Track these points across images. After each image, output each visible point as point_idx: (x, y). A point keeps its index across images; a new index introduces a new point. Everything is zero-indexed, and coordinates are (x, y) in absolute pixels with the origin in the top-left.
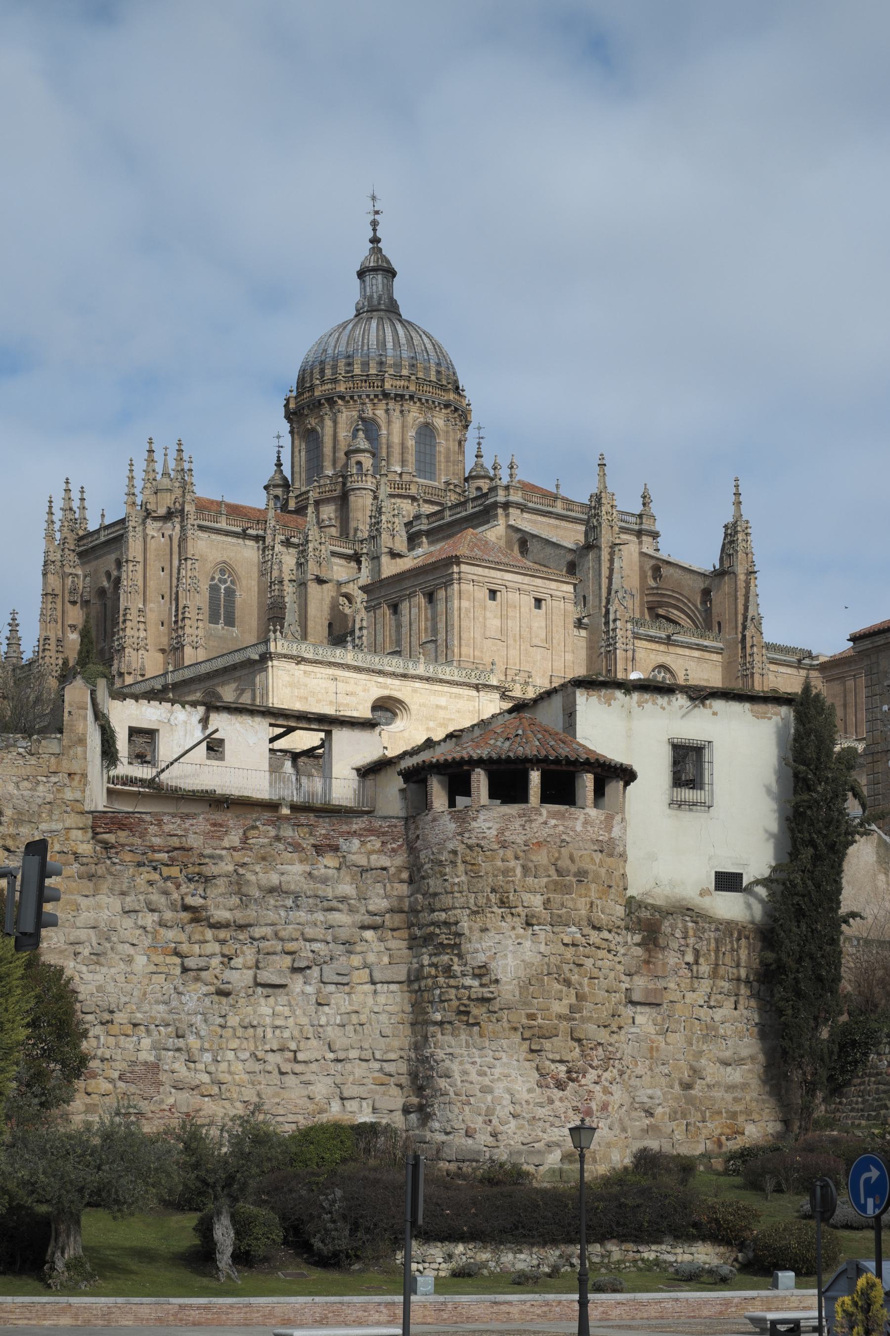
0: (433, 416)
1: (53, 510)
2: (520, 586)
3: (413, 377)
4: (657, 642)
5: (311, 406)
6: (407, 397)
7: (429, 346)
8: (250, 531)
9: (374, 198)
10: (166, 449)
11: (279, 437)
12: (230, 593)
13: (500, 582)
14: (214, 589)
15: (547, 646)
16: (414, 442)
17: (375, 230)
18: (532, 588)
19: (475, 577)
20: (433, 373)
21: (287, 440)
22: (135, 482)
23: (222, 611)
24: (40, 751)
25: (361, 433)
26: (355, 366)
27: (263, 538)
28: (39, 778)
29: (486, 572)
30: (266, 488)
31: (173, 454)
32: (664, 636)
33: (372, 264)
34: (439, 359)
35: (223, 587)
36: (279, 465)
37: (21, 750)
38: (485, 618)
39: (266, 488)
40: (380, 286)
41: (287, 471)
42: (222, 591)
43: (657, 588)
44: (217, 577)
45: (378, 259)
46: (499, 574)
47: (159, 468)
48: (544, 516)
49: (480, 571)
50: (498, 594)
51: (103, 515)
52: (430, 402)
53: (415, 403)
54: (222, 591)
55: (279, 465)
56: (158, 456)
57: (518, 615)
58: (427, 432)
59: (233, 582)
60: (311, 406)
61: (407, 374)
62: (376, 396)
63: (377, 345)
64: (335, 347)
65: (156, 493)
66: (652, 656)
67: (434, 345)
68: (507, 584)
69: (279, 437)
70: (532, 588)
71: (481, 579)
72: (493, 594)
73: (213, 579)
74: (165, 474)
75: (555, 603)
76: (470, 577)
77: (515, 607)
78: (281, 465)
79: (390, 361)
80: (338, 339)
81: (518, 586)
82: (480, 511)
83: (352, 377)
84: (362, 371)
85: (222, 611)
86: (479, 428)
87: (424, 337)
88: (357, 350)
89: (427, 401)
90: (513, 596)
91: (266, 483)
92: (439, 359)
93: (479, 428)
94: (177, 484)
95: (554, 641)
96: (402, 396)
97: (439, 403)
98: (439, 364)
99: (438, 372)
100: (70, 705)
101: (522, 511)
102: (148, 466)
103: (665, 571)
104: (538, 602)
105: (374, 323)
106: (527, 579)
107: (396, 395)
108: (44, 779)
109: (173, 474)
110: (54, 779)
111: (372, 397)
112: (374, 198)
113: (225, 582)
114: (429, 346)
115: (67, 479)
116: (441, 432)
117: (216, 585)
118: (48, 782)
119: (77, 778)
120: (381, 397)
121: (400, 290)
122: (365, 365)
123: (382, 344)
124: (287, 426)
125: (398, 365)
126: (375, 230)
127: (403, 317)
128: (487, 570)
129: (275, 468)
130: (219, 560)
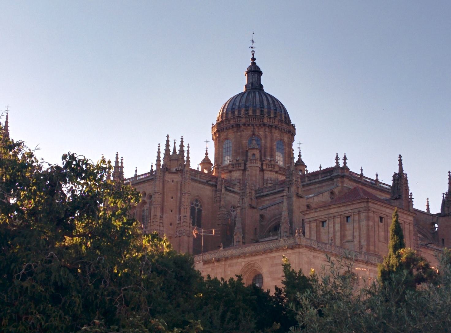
6: (274, 127)
7: (281, 105)
9: (253, 41)
12: (200, 211)
13: (384, 213)
17: (253, 55)
22: (160, 155)
26: (250, 111)
27: (216, 186)
33: (253, 69)
35: (197, 208)
36: (207, 154)
42: (196, 210)
47: (171, 149)
51: (136, 171)
54: (196, 210)
55: (207, 154)
56: (171, 144)
59: (201, 206)
64: (240, 103)
65: (170, 161)
71: (377, 210)
73: (192, 204)
74: (175, 152)
79: (266, 110)
83: (249, 116)
86: (300, 144)
96: (271, 126)
109: (178, 153)
111: (258, 125)
112: (253, 41)
113: (197, 205)
117: (193, 207)
120: (262, 126)
121: (264, 80)
122: (254, 111)
123: (262, 102)
125: (269, 113)
126: (253, 55)
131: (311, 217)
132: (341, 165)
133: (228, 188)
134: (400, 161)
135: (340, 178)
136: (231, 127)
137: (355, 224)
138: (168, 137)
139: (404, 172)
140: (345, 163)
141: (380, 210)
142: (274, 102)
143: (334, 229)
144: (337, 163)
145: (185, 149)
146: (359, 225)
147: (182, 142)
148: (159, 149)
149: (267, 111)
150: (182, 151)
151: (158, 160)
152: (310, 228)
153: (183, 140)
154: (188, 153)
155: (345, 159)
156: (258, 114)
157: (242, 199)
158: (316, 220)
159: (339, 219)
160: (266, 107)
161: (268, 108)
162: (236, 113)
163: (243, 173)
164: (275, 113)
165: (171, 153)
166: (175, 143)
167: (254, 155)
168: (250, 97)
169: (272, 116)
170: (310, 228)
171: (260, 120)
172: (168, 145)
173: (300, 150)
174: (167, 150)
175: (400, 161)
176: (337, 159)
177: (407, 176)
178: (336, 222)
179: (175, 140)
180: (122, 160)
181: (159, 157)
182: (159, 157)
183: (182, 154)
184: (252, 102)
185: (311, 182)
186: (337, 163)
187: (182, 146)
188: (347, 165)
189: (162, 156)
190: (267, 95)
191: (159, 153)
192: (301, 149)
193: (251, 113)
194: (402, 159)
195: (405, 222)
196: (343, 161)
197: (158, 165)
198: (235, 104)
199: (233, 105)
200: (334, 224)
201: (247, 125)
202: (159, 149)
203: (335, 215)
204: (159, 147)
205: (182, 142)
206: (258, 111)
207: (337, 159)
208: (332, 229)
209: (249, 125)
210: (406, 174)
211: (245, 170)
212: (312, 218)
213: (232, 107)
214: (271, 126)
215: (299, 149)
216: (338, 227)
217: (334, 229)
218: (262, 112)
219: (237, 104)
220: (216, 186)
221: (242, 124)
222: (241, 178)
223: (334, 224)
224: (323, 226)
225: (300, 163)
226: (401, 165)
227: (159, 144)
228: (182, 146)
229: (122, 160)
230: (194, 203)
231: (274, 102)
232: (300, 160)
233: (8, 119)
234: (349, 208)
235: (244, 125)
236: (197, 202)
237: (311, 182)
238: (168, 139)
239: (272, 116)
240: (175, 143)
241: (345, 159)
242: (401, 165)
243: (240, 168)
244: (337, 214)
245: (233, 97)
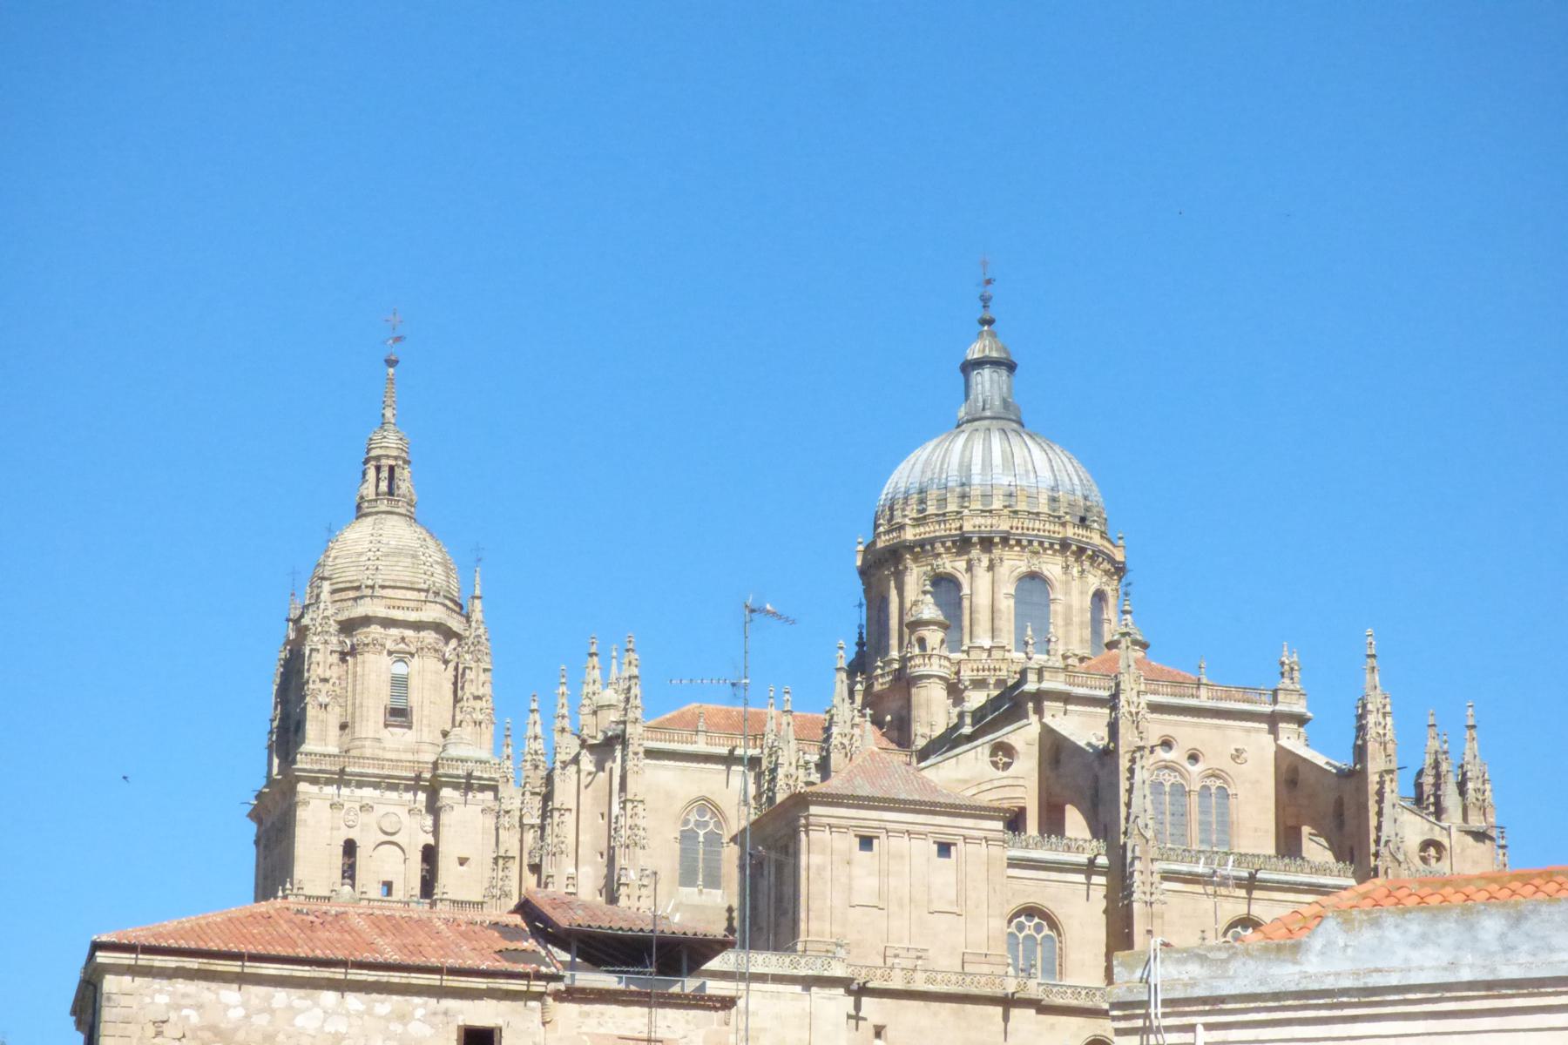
2: (910, 827)
8: (739, 752)
14: (687, 837)
16: (1012, 602)
23: (701, 865)
26: (929, 503)
34: (1056, 480)
35: (701, 833)
38: (850, 877)
40: (987, 385)
42: (701, 839)
44: (692, 820)
45: (985, 346)
52: (1036, 544)
54: (701, 839)
57: (907, 869)
59: (718, 824)
68: (889, 826)
71: (843, 822)
73: (686, 822)
76: (825, 820)
81: (905, 827)
84: (938, 508)
85: (701, 865)
92: (1056, 480)
104: (944, 849)
116: (1057, 584)
130: (694, 796)
195: (965, 838)
230: (693, 817)
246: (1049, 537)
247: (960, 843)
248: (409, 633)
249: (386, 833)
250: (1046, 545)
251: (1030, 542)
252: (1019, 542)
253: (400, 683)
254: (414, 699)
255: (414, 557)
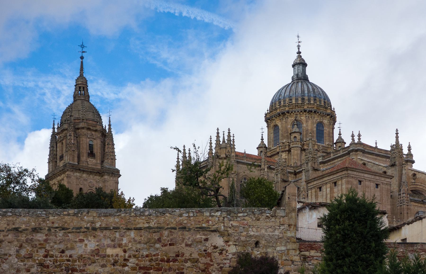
0: (323, 119)
1: (179, 157)
2: (370, 179)
3: (315, 104)
4: (418, 203)
5: (276, 116)
6: (313, 112)
7: (321, 92)
8: (256, 163)
10: (224, 132)
11: (262, 129)
13: (363, 177)
15: (381, 203)
16: (316, 129)
18: (375, 180)
19: (353, 176)
20: (323, 102)
21: (266, 130)
24: (276, 215)
25: (296, 126)
26: (293, 100)
27: (260, 166)
28: (276, 227)
29: (358, 174)
30: (257, 148)
31: (226, 134)
32: (420, 200)
34: (325, 97)
36: (262, 139)
37: (268, 215)
39: (257, 148)
41: (266, 142)
43: (415, 182)
46: (362, 175)
47: (221, 139)
48: (371, 155)
49: (355, 173)
50: (362, 182)
53: (316, 114)
55: (262, 139)
56: (221, 135)
57: (370, 191)
58: (320, 125)
60: (276, 116)
61: (313, 103)
62: (301, 111)
63: (301, 92)
64: (285, 93)
65: (220, 149)
66: (416, 208)
67: (323, 92)
68: (366, 178)
69: (262, 129)
70: (375, 180)
71: (356, 176)
72: (360, 182)
73: (241, 182)
74: (224, 141)
75: (384, 186)
77: (369, 187)
78: (263, 139)
79: (306, 98)
80: (286, 90)
82: (346, 153)
83: (292, 104)
84: (295, 102)
86: (340, 124)
87: (319, 89)
88: (294, 94)
89: (321, 113)
90: (367, 183)
91: (257, 147)
92: (325, 97)
93: (340, 124)
94: (228, 145)
95: (383, 201)
96: (311, 111)
97: (325, 114)
98: (325, 99)
99: (325, 102)
100: (289, 194)
101: (363, 153)
102: (217, 139)
103: (418, 176)
104: (377, 185)
105: (300, 84)
106: (373, 177)
107: (309, 111)
108: (278, 227)
109: (226, 141)
110: (282, 227)
111: (300, 112)
114: (321, 92)
115: (184, 145)
118: (280, 229)
119: (292, 227)
120: (303, 112)
122: (297, 100)
123: (303, 91)
124: (266, 124)
125: (309, 100)
127: (310, 81)
128: (358, 173)
129: (261, 141)
131: (312, 184)
132: (356, 141)
133: (272, 167)
134: (397, 134)
135: (354, 151)
136: (278, 115)
137: (339, 187)
138: (218, 130)
139: (400, 143)
140: (359, 139)
141: (358, 176)
142: (314, 90)
143: (326, 193)
144: (353, 140)
145: (232, 138)
146: (342, 188)
147: (229, 133)
148: (211, 141)
149: (307, 98)
150: (229, 140)
151: (211, 149)
152: (311, 193)
153: (230, 131)
154: (234, 142)
155: (359, 135)
156: (300, 102)
157: (277, 175)
158: (315, 187)
159: (329, 185)
160: (306, 95)
161: (308, 96)
162: (282, 103)
163: (288, 154)
164: (315, 100)
165: (221, 143)
166: (224, 134)
167: (295, 137)
168: (294, 87)
169: (312, 102)
170: (311, 193)
171: (301, 107)
172: (218, 137)
173: (340, 130)
174: (218, 140)
175: (397, 134)
176: (353, 136)
177: (402, 146)
178: (328, 187)
179: (224, 132)
180: (189, 150)
181: (211, 146)
182: (211, 146)
183: (229, 143)
184: (295, 92)
185: (335, 156)
186: (353, 140)
187: (229, 136)
188: (361, 140)
189: (214, 145)
190: (312, 84)
191: (211, 143)
192: (340, 128)
193: (294, 101)
194: (398, 132)
196: (358, 137)
197: (210, 153)
198: (282, 95)
199: (280, 96)
200: (326, 189)
201: (290, 113)
202: (211, 141)
203: (327, 182)
204: (211, 138)
205: (229, 133)
206: (300, 99)
207: (353, 136)
208: (325, 193)
209: (292, 112)
210: (402, 145)
211: (289, 151)
212: (312, 185)
213: (279, 97)
214: (310, 112)
215: (339, 128)
216: (328, 190)
217: (326, 193)
218: (303, 99)
219: (283, 95)
220: (261, 166)
221: (287, 112)
222: (287, 157)
223: (326, 189)
224: (320, 190)
225: (341, 141)
226: (397, 137)
227: (211, 136)
228: (229, 136)
229: (189, 150)
231: (314, 90)
232: (340, 138)
233: (111, 122)
234: (335, 176)
235: (288, 112)
236: (246, 180)
237: (335, 156)
238: (218, 131)
239: (312, 102)
240: (224, 134)
241: (359, 135)
242: (397, 137)
243: (286, 149)
244: (328, 181)
245: (279, 90)
246: (325, 112)
247: (381, 184)
248: (93, 133)
249: (90, 187)
250: (324, 114)
251: (321, 113)
252: (318, 113)
253: (91, 147)
254: (95, 151)
255: (93, 112)
